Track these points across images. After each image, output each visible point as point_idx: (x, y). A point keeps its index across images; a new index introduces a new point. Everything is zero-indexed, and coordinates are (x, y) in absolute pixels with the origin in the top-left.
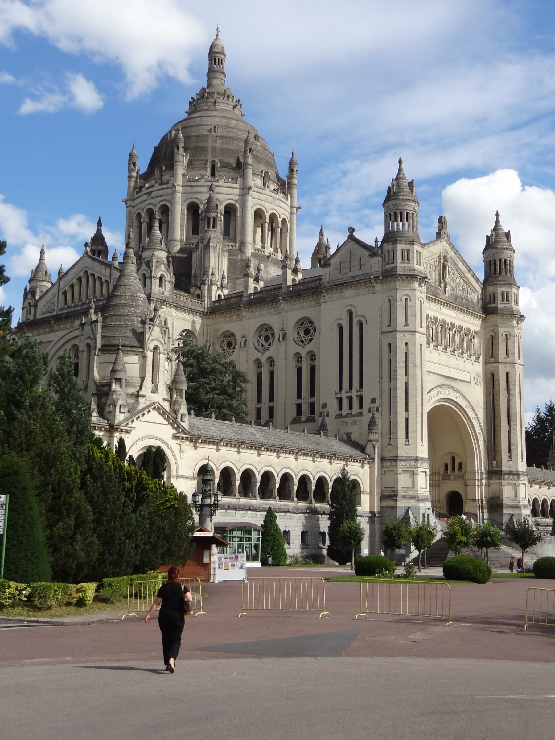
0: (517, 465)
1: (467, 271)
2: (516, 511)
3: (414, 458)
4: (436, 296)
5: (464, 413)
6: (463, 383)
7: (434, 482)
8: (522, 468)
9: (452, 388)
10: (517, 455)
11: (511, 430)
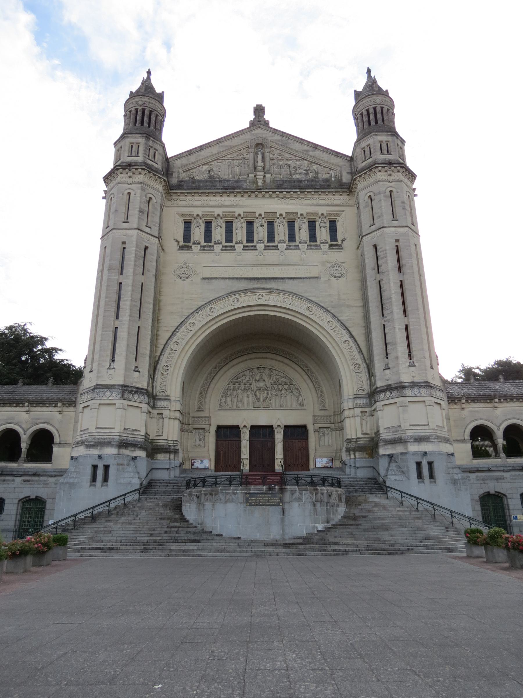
0: (398, 373)
1: (312, 149)
2: (399, 448)
3: (92, 388)
4: (222, 189)
5: (305, 319)
6: (296, 281)
7: (337, 425)
10: (397, 358)
11: (386, 323)
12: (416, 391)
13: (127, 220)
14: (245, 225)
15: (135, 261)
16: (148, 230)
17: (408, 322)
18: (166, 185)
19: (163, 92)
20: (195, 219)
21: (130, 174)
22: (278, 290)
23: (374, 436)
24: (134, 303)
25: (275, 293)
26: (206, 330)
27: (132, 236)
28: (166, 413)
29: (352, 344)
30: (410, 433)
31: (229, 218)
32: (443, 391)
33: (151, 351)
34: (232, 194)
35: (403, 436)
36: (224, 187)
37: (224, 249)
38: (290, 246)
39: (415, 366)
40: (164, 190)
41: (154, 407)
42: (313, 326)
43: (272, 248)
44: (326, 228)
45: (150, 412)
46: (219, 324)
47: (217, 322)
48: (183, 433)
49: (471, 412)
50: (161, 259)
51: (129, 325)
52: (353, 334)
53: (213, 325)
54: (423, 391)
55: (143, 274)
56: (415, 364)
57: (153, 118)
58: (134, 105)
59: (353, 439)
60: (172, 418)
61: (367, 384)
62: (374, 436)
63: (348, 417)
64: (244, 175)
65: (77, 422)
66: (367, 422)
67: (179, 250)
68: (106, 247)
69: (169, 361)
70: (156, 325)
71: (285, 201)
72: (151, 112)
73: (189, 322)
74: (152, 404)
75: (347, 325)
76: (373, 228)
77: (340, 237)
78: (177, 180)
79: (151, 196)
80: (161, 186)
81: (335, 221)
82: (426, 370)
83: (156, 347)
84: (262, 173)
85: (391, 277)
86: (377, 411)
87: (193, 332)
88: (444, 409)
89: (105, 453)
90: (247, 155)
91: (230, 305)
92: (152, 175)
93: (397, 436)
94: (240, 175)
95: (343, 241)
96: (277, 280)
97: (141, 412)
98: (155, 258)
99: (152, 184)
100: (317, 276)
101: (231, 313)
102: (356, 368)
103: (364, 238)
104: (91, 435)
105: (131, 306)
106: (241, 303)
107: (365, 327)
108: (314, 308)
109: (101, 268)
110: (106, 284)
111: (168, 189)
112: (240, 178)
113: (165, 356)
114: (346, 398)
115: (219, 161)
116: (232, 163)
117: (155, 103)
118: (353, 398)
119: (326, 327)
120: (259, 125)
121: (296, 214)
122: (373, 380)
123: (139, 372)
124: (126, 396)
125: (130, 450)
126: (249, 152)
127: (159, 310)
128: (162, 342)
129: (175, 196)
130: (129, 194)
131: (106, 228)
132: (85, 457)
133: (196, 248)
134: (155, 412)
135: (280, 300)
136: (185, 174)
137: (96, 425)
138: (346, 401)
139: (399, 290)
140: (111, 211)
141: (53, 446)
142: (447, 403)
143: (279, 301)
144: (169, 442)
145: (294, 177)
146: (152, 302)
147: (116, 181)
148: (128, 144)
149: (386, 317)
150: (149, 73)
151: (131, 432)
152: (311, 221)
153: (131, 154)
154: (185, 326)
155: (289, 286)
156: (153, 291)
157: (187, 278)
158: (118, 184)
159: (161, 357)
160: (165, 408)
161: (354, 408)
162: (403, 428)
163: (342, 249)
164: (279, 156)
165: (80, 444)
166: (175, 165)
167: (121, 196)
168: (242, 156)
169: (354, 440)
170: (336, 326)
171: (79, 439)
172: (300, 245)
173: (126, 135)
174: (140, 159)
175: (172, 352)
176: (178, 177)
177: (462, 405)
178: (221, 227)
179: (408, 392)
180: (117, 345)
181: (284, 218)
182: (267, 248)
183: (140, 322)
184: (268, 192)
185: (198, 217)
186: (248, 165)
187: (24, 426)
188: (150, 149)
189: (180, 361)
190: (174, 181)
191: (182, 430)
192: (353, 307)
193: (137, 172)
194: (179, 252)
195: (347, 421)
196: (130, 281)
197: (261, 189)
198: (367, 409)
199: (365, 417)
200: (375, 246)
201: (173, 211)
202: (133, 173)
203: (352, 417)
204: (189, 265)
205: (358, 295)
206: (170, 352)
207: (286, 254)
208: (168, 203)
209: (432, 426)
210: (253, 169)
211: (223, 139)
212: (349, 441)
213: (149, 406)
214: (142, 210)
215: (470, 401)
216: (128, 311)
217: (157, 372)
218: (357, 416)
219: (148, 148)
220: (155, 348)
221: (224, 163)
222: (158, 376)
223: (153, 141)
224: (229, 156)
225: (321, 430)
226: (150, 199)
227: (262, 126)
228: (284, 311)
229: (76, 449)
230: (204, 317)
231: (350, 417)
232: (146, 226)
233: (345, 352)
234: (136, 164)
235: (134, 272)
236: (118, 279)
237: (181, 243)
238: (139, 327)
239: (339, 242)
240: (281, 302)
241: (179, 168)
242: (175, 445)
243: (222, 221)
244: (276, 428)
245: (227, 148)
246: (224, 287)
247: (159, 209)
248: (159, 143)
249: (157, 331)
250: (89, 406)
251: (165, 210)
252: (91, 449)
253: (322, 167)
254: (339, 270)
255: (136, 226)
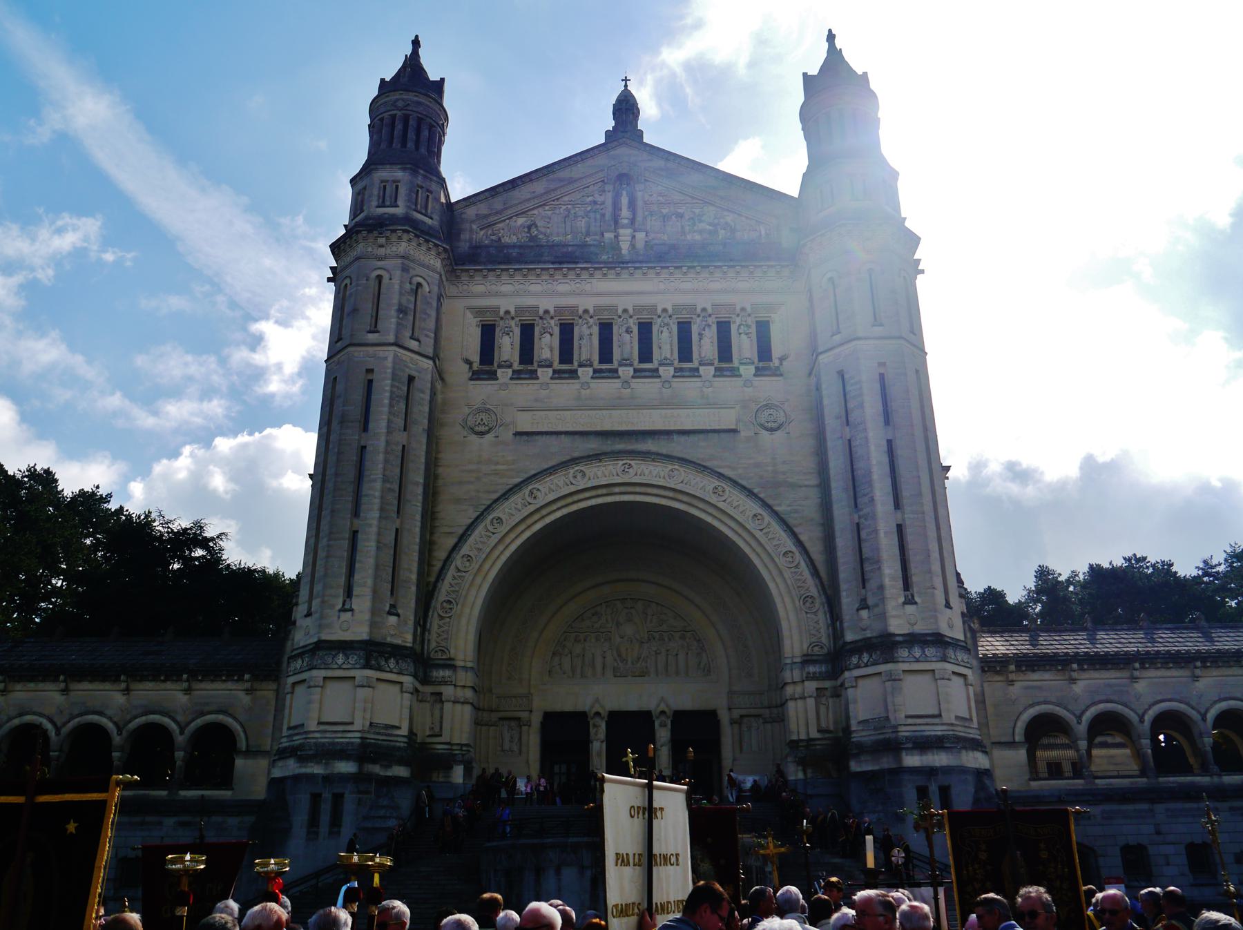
0: (883, 616)
2: (885, 760)
3: (311, 647)
4: (553, 263)
5: (710, 510)
6: (693, 438)
7: (775, 711)
8: (951, 627)
9: (646, 455)
10: (881, 588)
12: (917, 652)
13: (376, 327)
14: (596, 330)
15: (391, 406)
16: (413, 344)
17: (904, 520)
18: (449, 258)
19: (442, 80)
20: (502, 318)
21: (382, 241)
22: (658, 454)
23: (841, 734)
24: (388, 486)
25: (653, 460)
26: (522, 532)
27: (386, 358)
28: (448, 691)
29: (798, 557)
30: (904, 732)
31: (567, 318)
32: (969, 650)
33: (420, 574)
34: (572, 272)
35: (893, 736)
36: (558, 257)
37: (557, 376)
38: (681, 370)
39: (916, 603)
40: (444, 266)
41: (425, 681)
42: (726, 524)
43: (647, 374)
44: (750, 335)
45: (417, 690)
46: (548, 520)
47: (543, 517)
48: (479, 727)
49: (1027, 688)
50: (439, 397)
51: (379, 528)
52: (803, 538)
53: (536, 522)
54: (930, 651)
55: (405, 430)
56: (917, 599)
57: (426, 133)
58: (389, 108)
59: (802, 740)
60: (458, 702)
61: (829, 635)
62: (841, 734)
63: (791, 699)
64: (596, 234)
65: (283, 710)
66: (828, 708)
67: (471, 379)
68: (335, 379)
69: (453, 591)
70: (429, 525)
71: (672, 284)
72: (420, 121)
73: (491, 517)
74: (421, 674)
75: (791, 521)
76: (837, 338)
77: (777, 352)
78: (468, 244)
79: (420, 280)
80: (439, 261)
81: (768, 322)
82: (935, 610)
83: (430, 565)
84: (629, 231)
85: (871, 434)
86: (846, 689)
87: (498, 536)
88: (971, 685)
89: (336, 771)
90: (600, 195)
91: (569, 483)
92: (421, 240)
93: (881, 737)
94: (588, 234)
95: (782, 359)
96: (656, 437)
97: (402, 692)
98: (427, 397)
99: (422, 258)
100: (734, 427)
101: (570, 500)
102: (808, 604)
103: (821, 357)
104: (309, 736)
105: (382, 491)
106: (589, 479)
107: (823, 525)
108: (727, 489)
109: (326, 418)
110: (336, 450)
111: (451, 264)
112: (588, 239)
113: (446, 582)
114: (788, 661)
115: (547, 208)
116: (572, 212)
117: (428, 103)
118: (801, 663)
119: (750, 525)
120: (624, 140)
121: (692, 309)
122: (838, 628)
123: (398, 615)
124: (373, 662)
125: (381, 766)
126: (604, 191)
127: (435, 494)
128: (441, 554)
129: (464, 277)
130: (380, 278)
131: (336, 342)
132: (296, 778)
133: (504, 375)
134: (429, 689)
135: (662, 474)
136: (482, 232)
137: (319, 718)
138: (788, 666)
139: (885, 459)
140: (347, 310)
141: (235, 756)
142: (980, 671)
143: (662, 476)
144: (455, 747)
145: (689, 237)
146: (422, 481)
147: (355, 253)
148: (377, 182)
149: (861, 510)
150: (416, 43)
151: (382, 731)
152: (722, 322)
153: (383, 201)
154: (483, 524)
155: (676, 447)
156: (423, 460)
157: (488, 432)
158: (357, 259)
159: (439, 585)
160: (445, 682)
161: (803, 681)
162: (893, 722)
163: (781, 375)
164: (661, 198)
165: (288, 755)
166: (463, 216)
167: (365, 282)
168: (590, 198)
169: (805, 744)
170: (769, 524)
171: (285, 743)
172: (701, 368)
173: (372, 167)
174: (399, 211)
175: (459, 574)
176: (471, 240)
177: (1010, 675)
178: (551, 335)
179: (903, 653)
180: (357, 565)
181: (670, 316)
182: (638, 374)
183: (398, 522)
184: (641, 268)
185: (508, 316)
186: (603, 215)
187: (179, 718)
188: (418, 191)
189: (473, 592)
190: (463, 246)
191: (477, 723)
192: (801, 487)
193: (394, 237)
194: (472, 382)
195: (791, 704)
196: (382, 444)
197: (627, 263)
198: (827, 684)
199: (824, 698)
200: (841, 374)
201: (460, 304)
202: (388, 238)
203: (801, 698)
204: (490, 407)
205: (810, 464)
206: (455, 574)
207: (674, 385)
208: (451, 290)
209: (949, 717)
210: (612, 223)
211: (556, 166)
212: (794, 744)
213: (417, 679)
214: (404, 309)
215: (1024, 669)
216: (377, 501)
217: (430, 614)
218: (810, 697)
219: (414, 190)
220: (426, 568)
221: (557, 212)
222: (434, 623)
223: (425, 177)
224: (566, 199)
225: (745, 720)
226: (419, 285)
227: (628, 142)
228: (671, 494)
229: (280, 764)
230: (519, 507)
231: (796, 699)
232: (411, 338)
233: (787, 574)
234: (394, 219)
235: (388, 427)
236: (359, 441)
237: (476, 366)
238: (397, 530)
239: (776, 362)
240: (664, 478)
241: (472, 222)
242: (464, 752)
243: (552, 322)
244: (657, 718)
245: (562, 184)
246: (559, 449)
247: (435, 304)
248: (435, 178)
249: (432, 534)
250: (304, 681)
251: (445, 302)
252: (310, 764)
253: (743, 219)
254: (774, 414)
255: (391, 339)
